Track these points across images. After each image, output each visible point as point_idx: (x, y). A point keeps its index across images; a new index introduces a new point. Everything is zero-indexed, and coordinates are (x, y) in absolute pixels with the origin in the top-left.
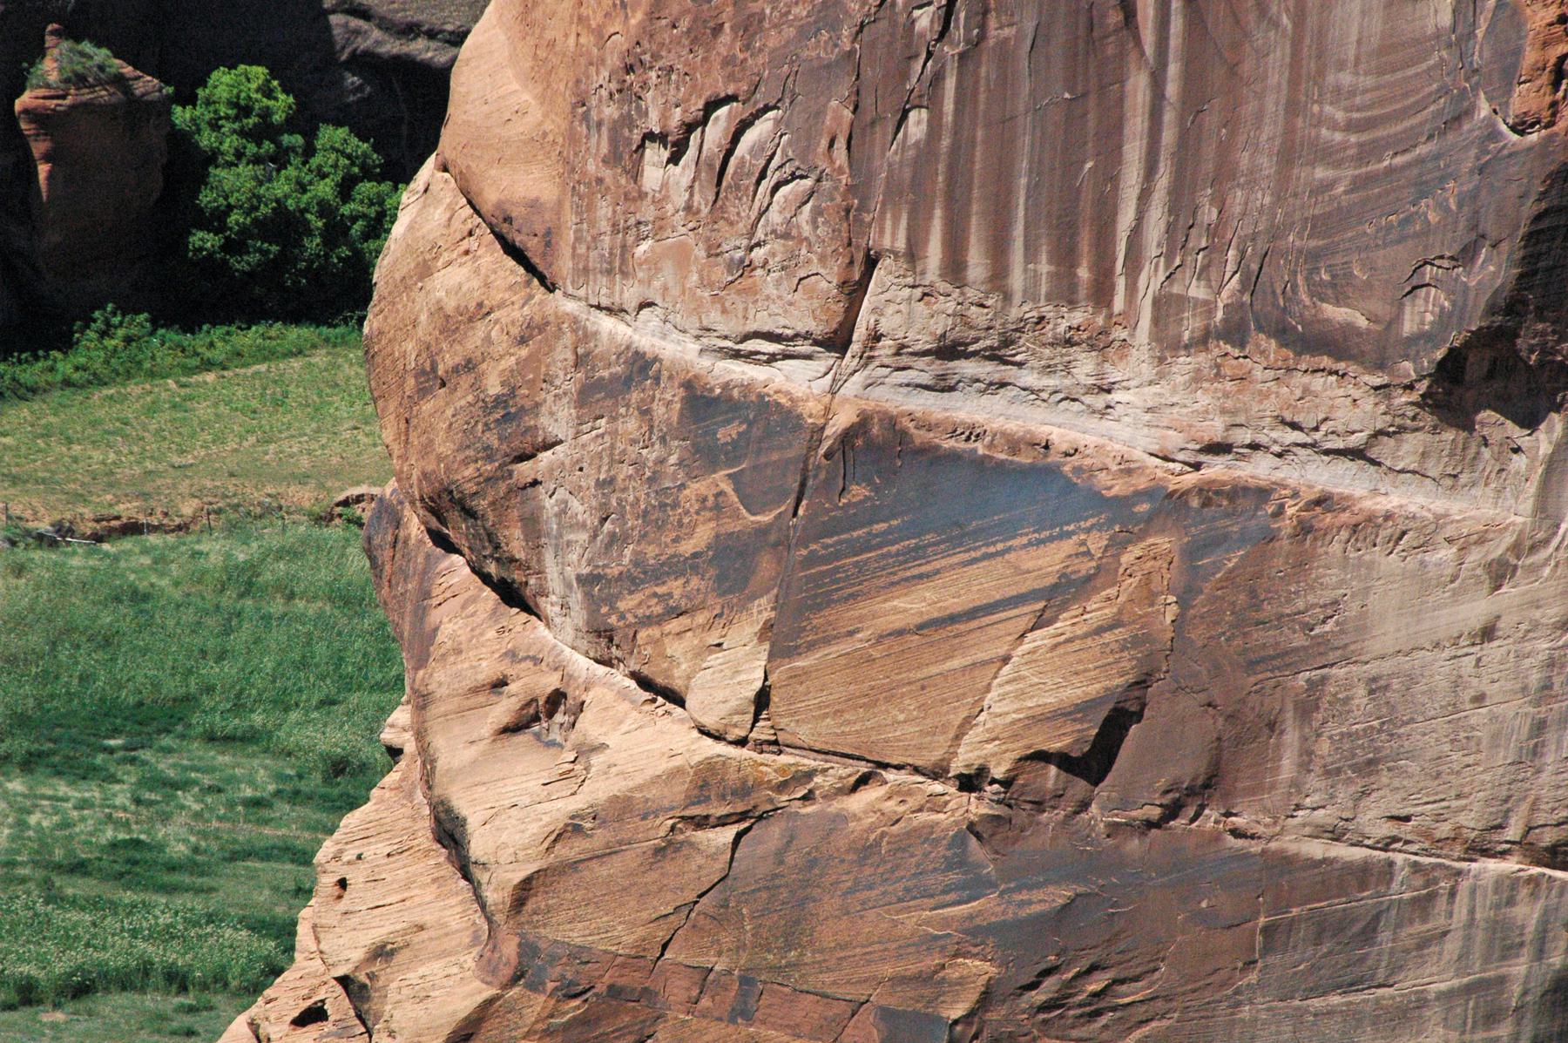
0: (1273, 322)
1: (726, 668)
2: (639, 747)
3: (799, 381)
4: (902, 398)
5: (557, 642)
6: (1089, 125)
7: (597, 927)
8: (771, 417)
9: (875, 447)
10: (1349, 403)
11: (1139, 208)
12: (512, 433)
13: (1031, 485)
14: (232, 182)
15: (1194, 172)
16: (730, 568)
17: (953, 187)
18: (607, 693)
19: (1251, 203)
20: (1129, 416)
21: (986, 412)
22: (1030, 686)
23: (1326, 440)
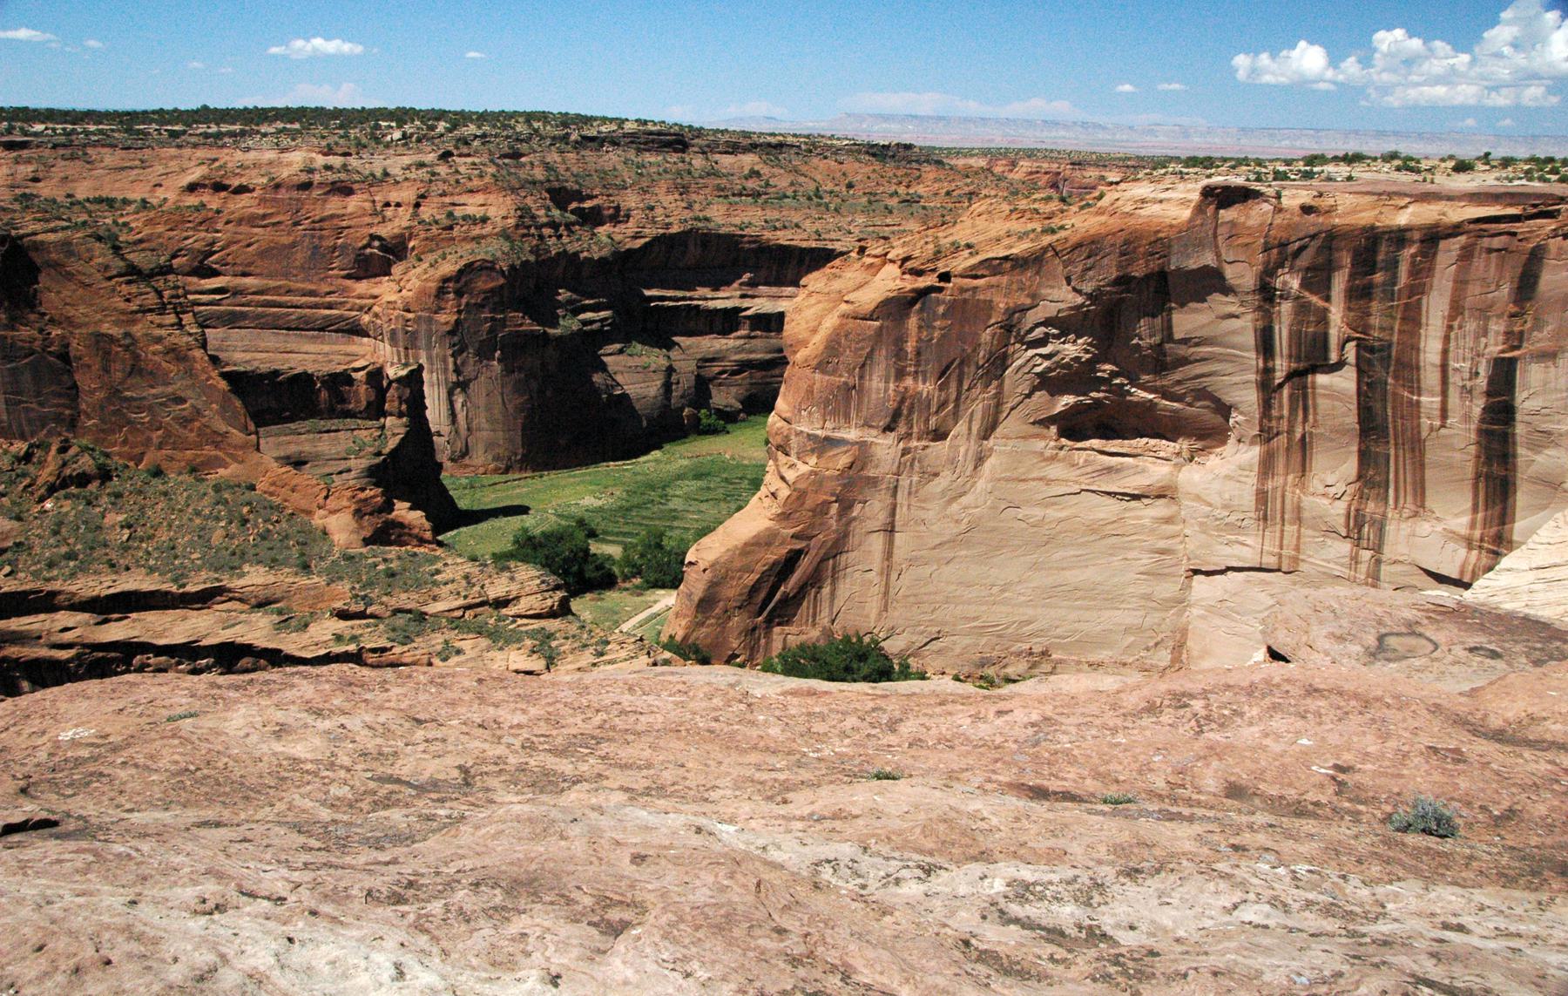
0: (867, 424)
1: (813, 460)
2: (803, 469)
3: (819, 432)
4: (829, 434)
5: (793, 459)
6: (848, 406)
7: (802, 486)
8: (816, 436)
9: (827, 438)
10: (874, 432)
11: (853, 414)
12: (787, 438)
13: (842, 442)
14: (704, 421)
15: (859, 410)
16: (813, 451)
17: (834, 413)
18: (799, 464)
19: (864, 413)
20: (852, 434)
21: (837, 435)
22: (844, 461)
23: (871, 436)
